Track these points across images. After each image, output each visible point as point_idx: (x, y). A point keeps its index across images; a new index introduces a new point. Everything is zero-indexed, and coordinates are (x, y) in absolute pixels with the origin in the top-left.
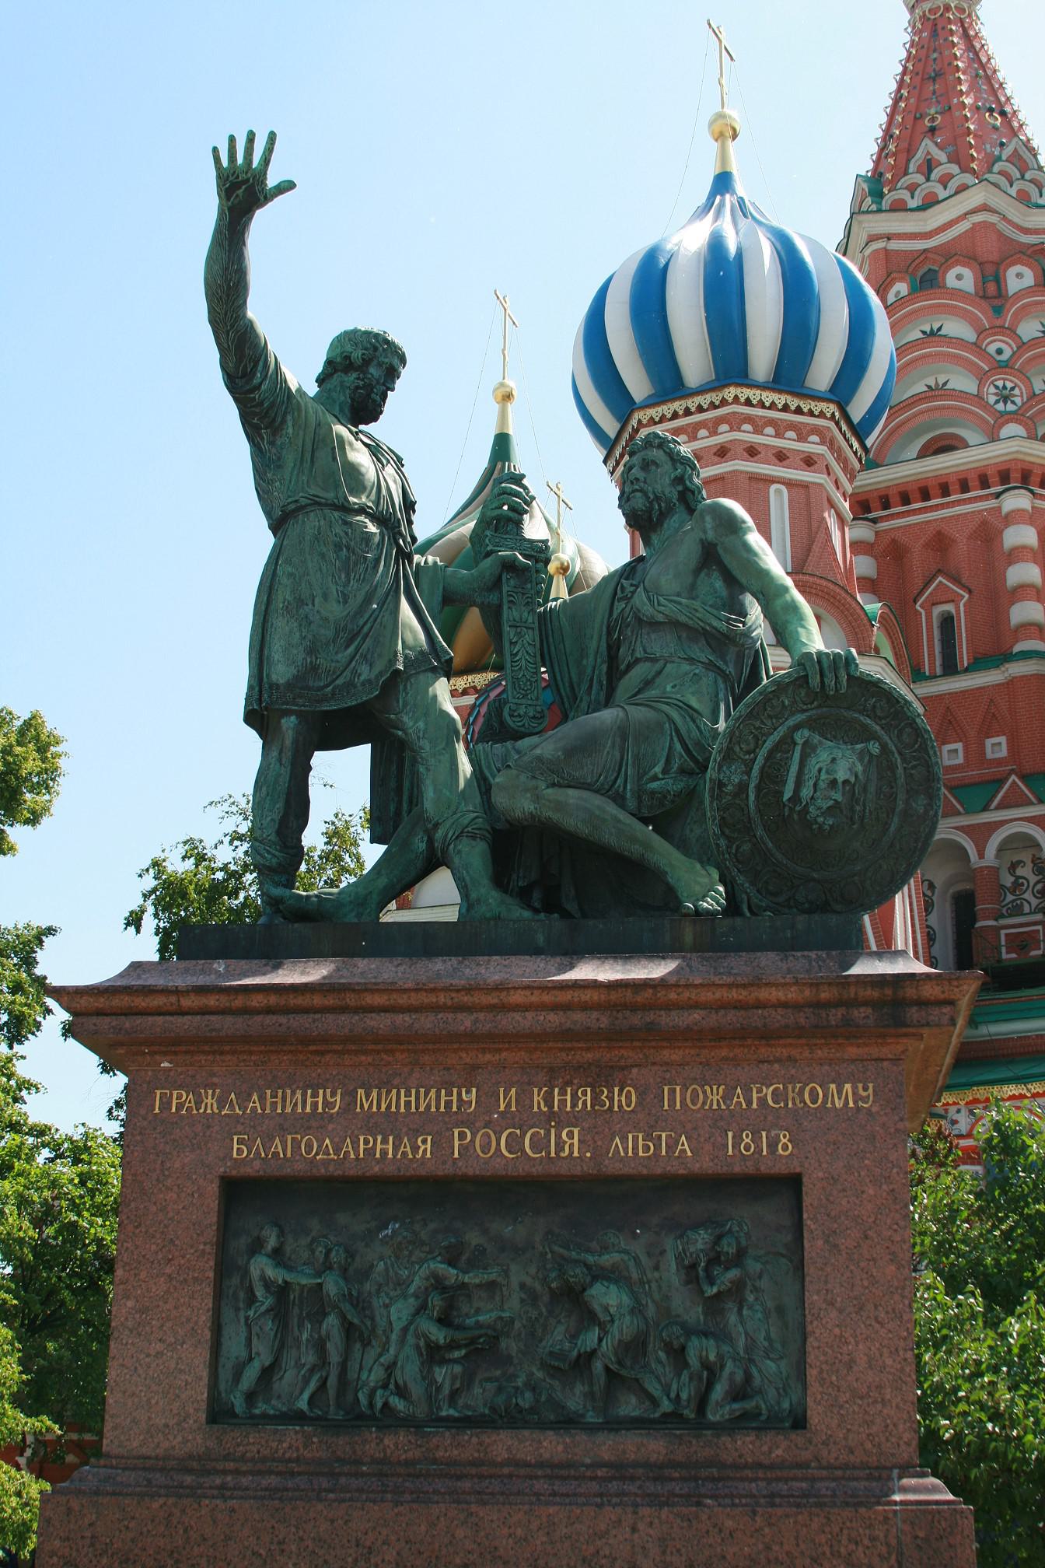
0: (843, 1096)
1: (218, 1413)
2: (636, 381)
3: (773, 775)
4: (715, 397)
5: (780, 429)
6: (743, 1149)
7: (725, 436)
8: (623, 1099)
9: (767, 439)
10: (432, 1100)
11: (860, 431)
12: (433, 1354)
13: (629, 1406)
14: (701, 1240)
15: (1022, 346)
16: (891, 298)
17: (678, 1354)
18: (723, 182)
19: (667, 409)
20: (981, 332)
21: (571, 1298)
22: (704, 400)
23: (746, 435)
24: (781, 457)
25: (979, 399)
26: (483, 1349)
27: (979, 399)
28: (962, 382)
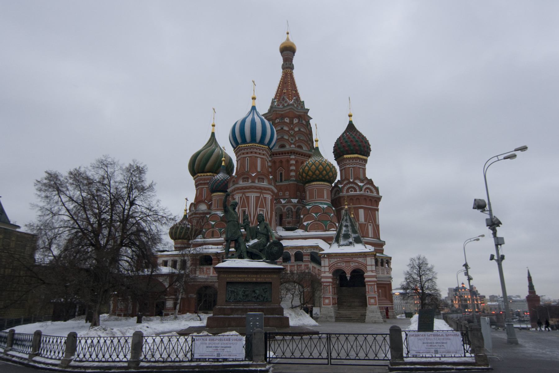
0: (275, 276)
1: (226, 301)
2: (239, 140)
3: (271, 249)
4: (251, 144)
5: (260, 150)
6: (267, 280)
7: (252, 150)
8: (258, 276)
9: (258, 151)
10: (244, 276)
11: (271, 149)
12: (243, 296)
13: (258, 300)
14: (264, 287)
15: (295, 132)
16: (276, 122)
17: (262, 296)
18: (254, 108)
19: (244, 145)
20: (290, 129)
21: (254, 291)
22: (249, 145)
23: (255, 150)
24: (260, 154)
25: (288, 140)
26: (247, 296)
27: (288, 140)
28: (286, 137)
